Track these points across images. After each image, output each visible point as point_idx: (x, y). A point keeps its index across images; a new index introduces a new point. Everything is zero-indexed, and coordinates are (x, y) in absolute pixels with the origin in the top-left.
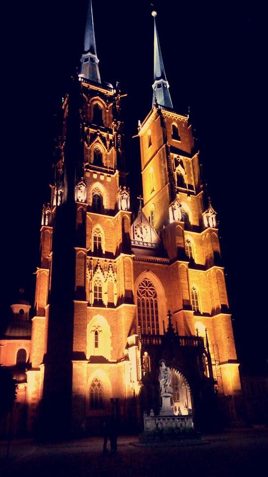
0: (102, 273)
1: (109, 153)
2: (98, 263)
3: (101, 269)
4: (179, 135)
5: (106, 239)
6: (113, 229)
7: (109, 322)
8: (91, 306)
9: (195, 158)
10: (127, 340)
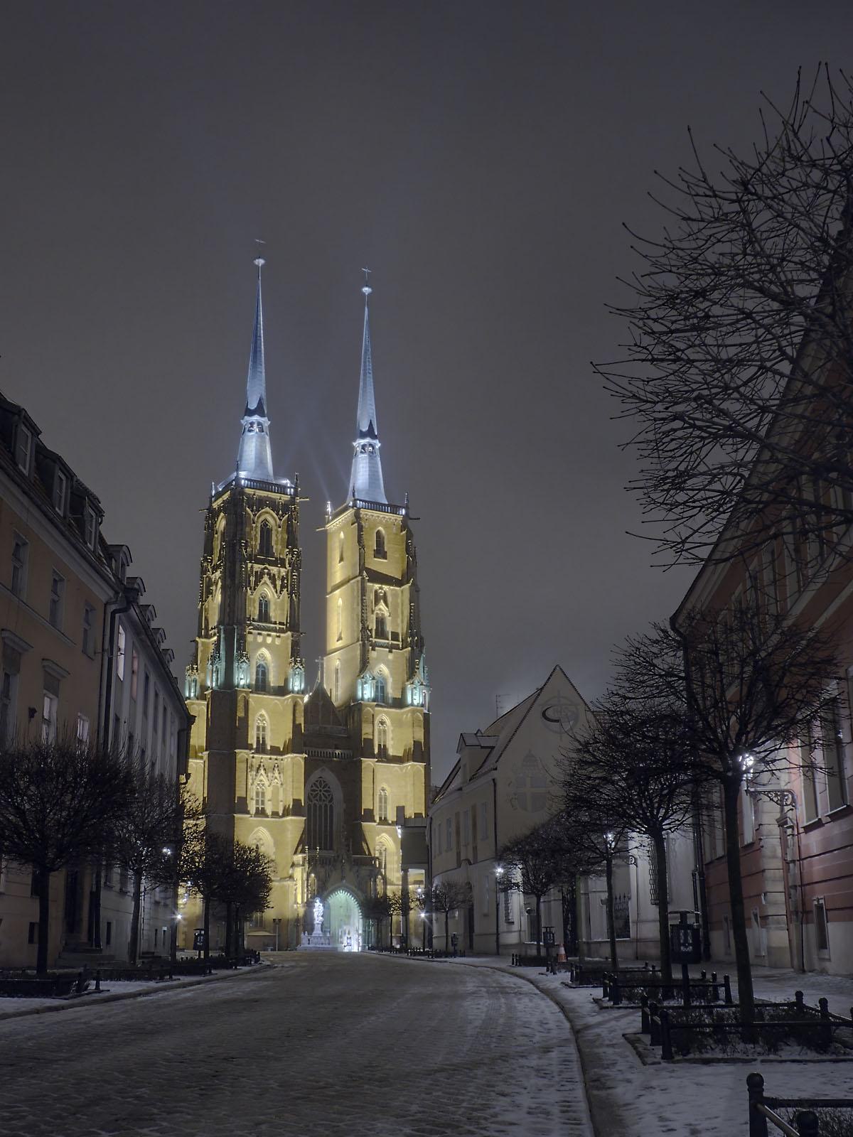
0: (265, 776)
1: (278, 600)
2: (261, 762)
3: (265, 769)
4: (386, 550)
5: (271, 730)
7: (272, 835)
10: (292, 858)
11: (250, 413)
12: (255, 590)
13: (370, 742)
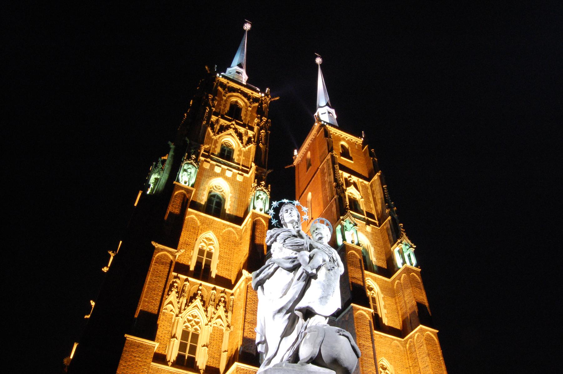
0: (202, 309)
2: (199, 290)
5: (220, 257)
6: (237, 244)
8: (168, 365)
9: (375, 180)
12: (218, 133)
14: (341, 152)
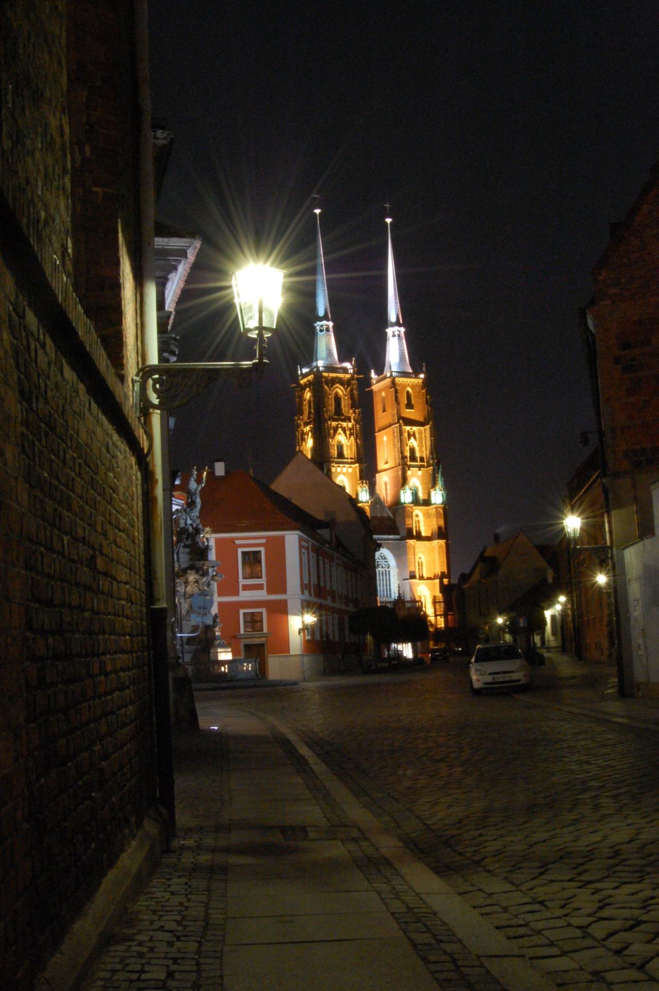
11: (321, 319)
13: (410, 530)
14: (406, 402)
